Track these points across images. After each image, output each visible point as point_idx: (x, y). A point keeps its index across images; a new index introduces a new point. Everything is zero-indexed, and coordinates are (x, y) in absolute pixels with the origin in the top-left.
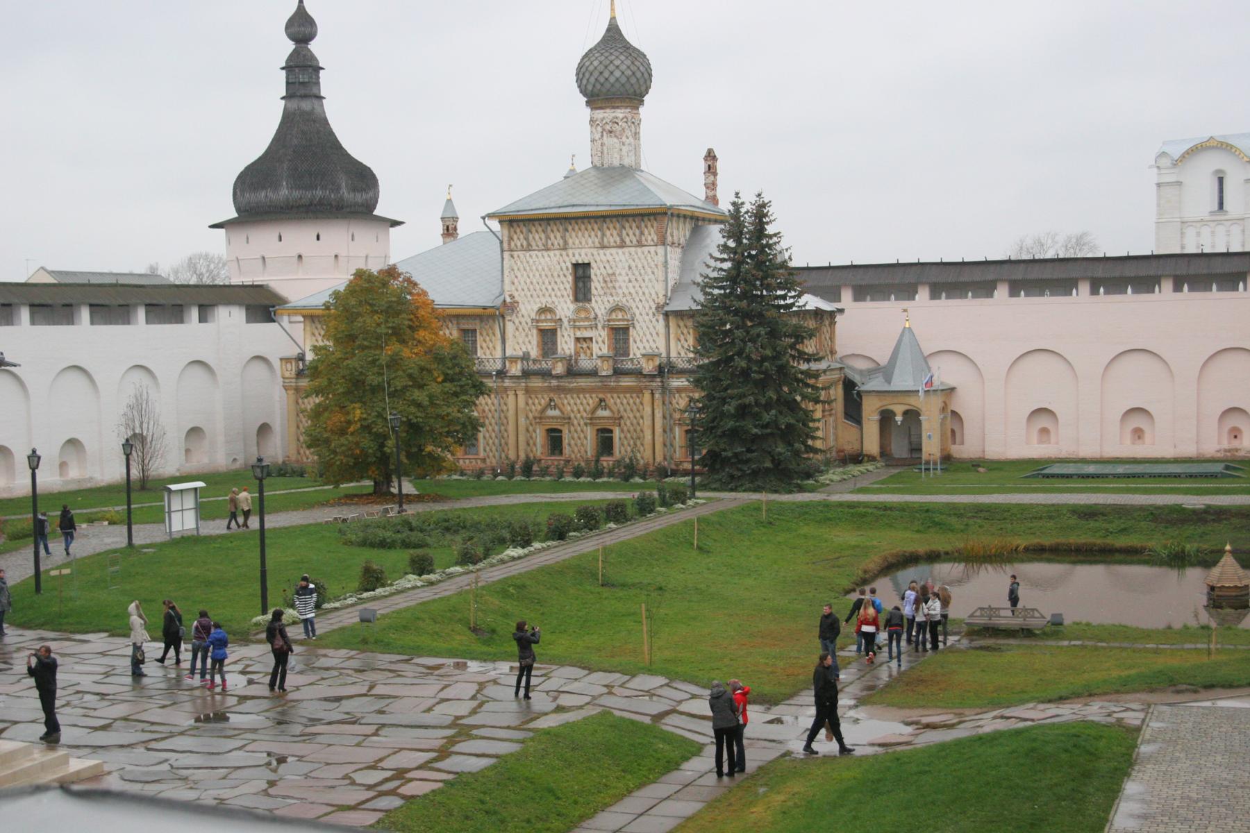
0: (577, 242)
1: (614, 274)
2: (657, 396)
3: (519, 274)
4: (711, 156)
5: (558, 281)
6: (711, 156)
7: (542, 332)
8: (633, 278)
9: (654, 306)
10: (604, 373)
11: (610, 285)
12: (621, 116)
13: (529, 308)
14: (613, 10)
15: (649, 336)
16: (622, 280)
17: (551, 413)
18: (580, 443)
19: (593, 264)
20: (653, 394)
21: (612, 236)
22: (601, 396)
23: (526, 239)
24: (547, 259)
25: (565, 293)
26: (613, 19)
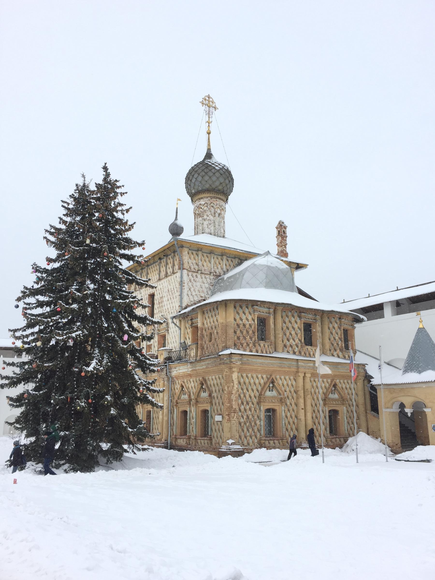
12: (203, 203)
14: (209, 145)
26: (209, 150)
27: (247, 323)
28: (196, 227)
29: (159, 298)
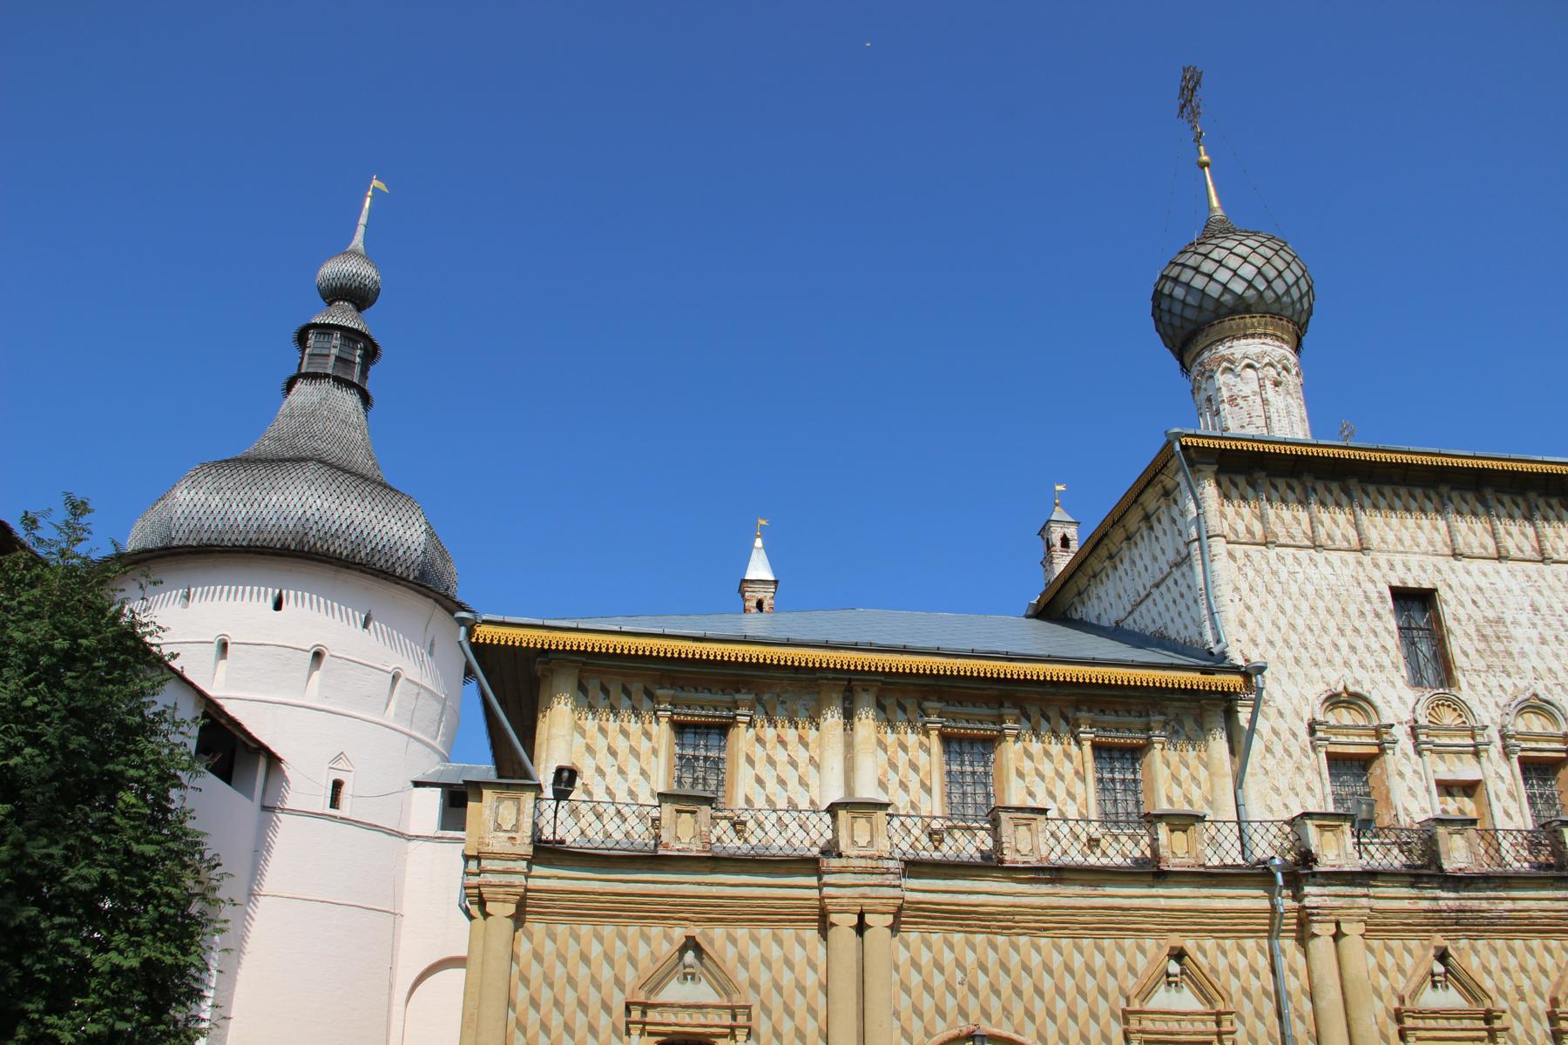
0: (1391, 537)
1: (1500, 621)
3: (1254, 602)
5: (1363, 628)
7: (1340, 764)
11: (1497, 646)
13: (1294, 692)
16: (1523, 636)
17: (1433, 999)
19: (1443, 592)
21: (1472, 531)
23: (1262, 518)
24: (1327, 570)
29: (1481, 621)
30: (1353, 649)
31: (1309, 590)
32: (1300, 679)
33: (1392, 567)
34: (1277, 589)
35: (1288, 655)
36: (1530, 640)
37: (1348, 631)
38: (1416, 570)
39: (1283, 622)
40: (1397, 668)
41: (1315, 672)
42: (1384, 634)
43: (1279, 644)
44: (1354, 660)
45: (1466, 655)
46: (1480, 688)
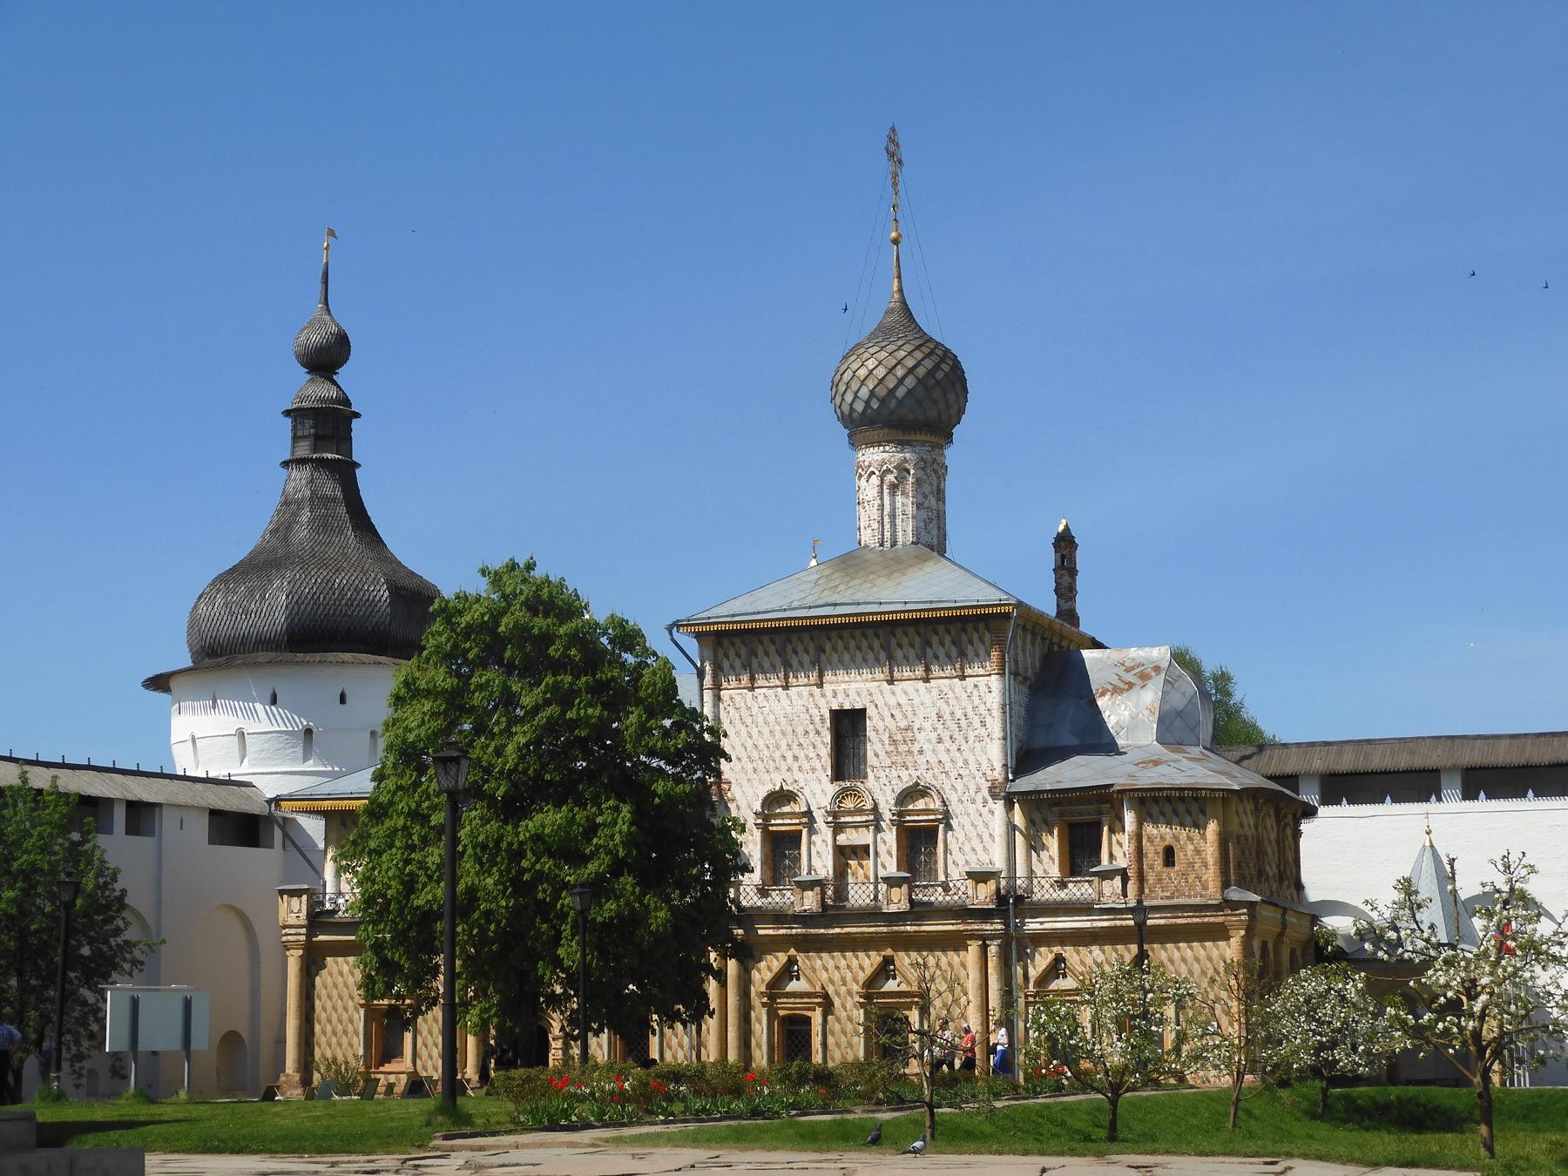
2: (993, 950)
4: (1065, 544)
6: (1065, 544)
8: (945, 736)
9: (985, 786)
10: (893, 909)
15: (975, 842)
18: (842, 1040)
19: (871, 712)
20: (984, 948)
22: (889, 952)
24: (785, 702)
25: (818, 766)
27: (1249, 833)
28: (887, 519)
29: (894, 729)
30: (796, 758)
31: (771, 718)
32: (755, 783)
33: (835, 695)
34: (749, 721)
35: (749, 766)
36: (929, 741)
37: (795, 746)
38: (853, 695)
39: (749, 744)
40: (825, 770)
41: (766, 777)
42: (820, 746)
43: (745, 759)
44: (795, 766)
45: (877, 755)
46: (884, 780)
